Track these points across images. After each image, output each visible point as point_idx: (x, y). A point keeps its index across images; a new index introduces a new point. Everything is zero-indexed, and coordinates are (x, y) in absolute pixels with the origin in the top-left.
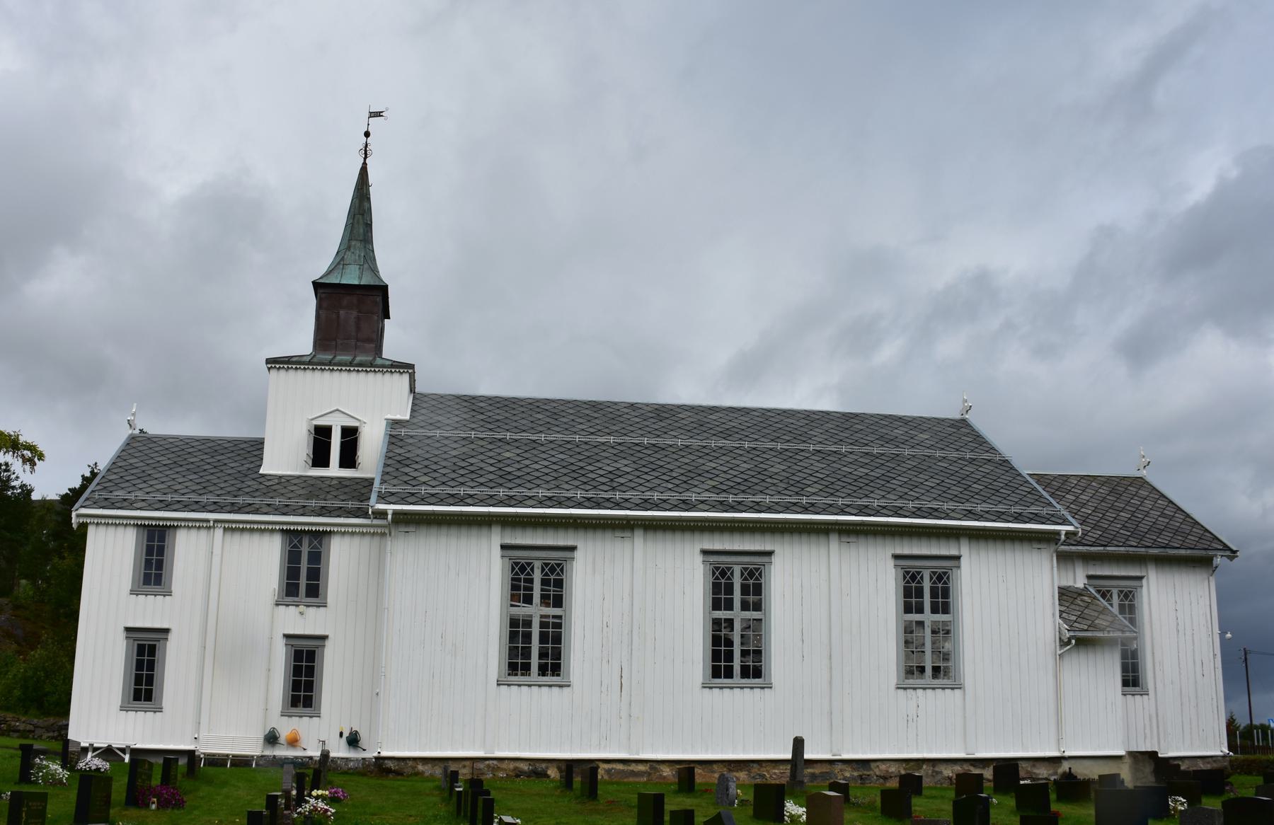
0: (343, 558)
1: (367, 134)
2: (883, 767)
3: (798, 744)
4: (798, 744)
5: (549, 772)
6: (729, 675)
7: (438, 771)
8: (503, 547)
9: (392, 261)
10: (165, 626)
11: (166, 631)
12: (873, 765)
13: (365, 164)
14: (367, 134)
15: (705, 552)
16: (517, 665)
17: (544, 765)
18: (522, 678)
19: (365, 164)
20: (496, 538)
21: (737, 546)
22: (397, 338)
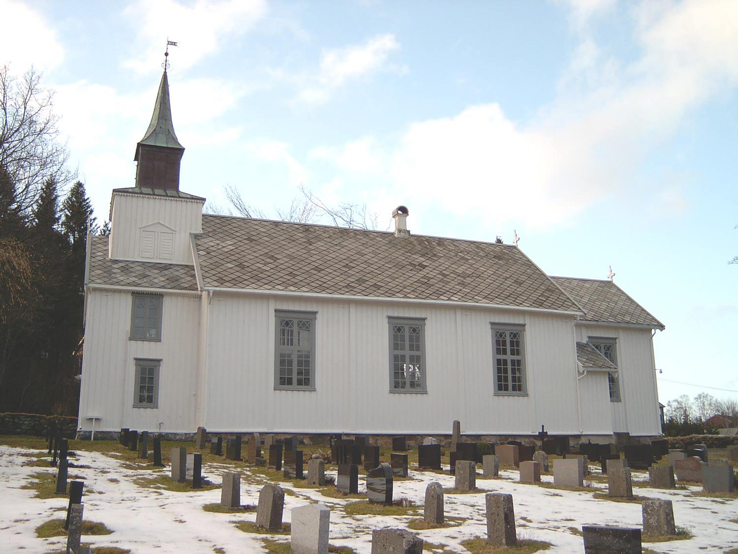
0: (173, 312)
1: (167, 54)
2: (488, 439)
3: (457, 425)
4: (457, 425)
5: (304, 441)
6: (506, 389)
7: (234, 437)
8: (276, 311)
9: (184, 132)
10: (158, 358)
11: (159, 361)
12: (482, 437)
13: (165, 72)
14: (167, 54)
15: (389, 318)
16: (284, 380)
17: (301, 437)
18: (288, 386)
19: (165, 72)
20: (273, 306)
21: (407, 315)
22: (189, 180)
